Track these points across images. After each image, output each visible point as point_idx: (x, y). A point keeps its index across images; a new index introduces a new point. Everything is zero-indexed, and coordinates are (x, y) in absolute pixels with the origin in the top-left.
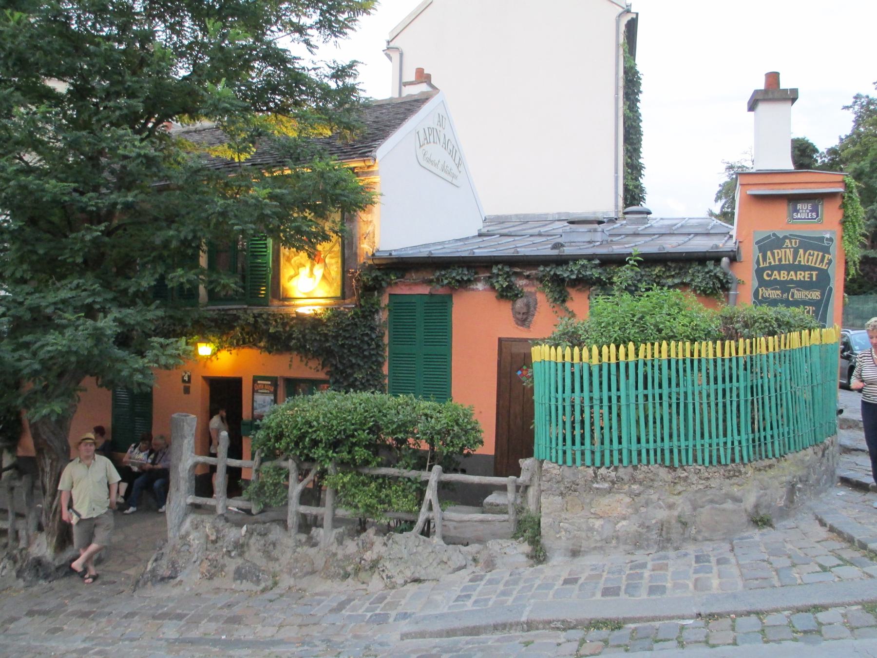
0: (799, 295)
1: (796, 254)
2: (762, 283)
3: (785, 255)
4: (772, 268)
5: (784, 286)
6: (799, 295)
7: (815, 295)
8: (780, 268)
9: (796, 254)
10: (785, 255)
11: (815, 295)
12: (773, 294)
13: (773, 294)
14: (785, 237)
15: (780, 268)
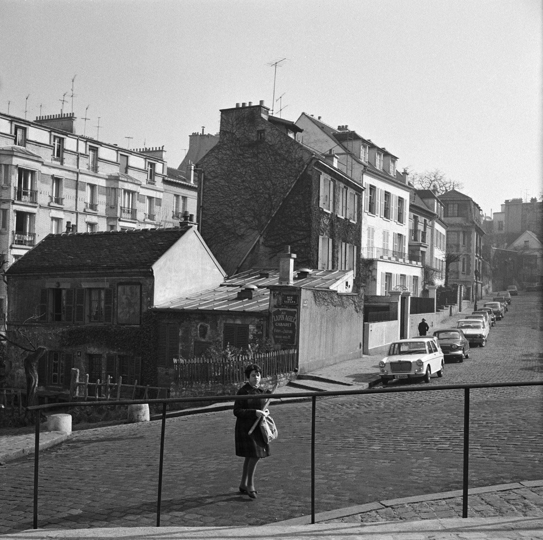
0: (286, 332)
1: (285, 317)
2: (275, 327)
3: (282, 317)
4: (278, 322)
5: (281, 328)
6: (286, 332)
7: (291, 332)
8: (280, 322)
9: (285, 317)
10: (282, 317)
11: (291, 332)
12: (278, 331)
13: (278, 331)
14: (282, 311)
15: (280, 322)
